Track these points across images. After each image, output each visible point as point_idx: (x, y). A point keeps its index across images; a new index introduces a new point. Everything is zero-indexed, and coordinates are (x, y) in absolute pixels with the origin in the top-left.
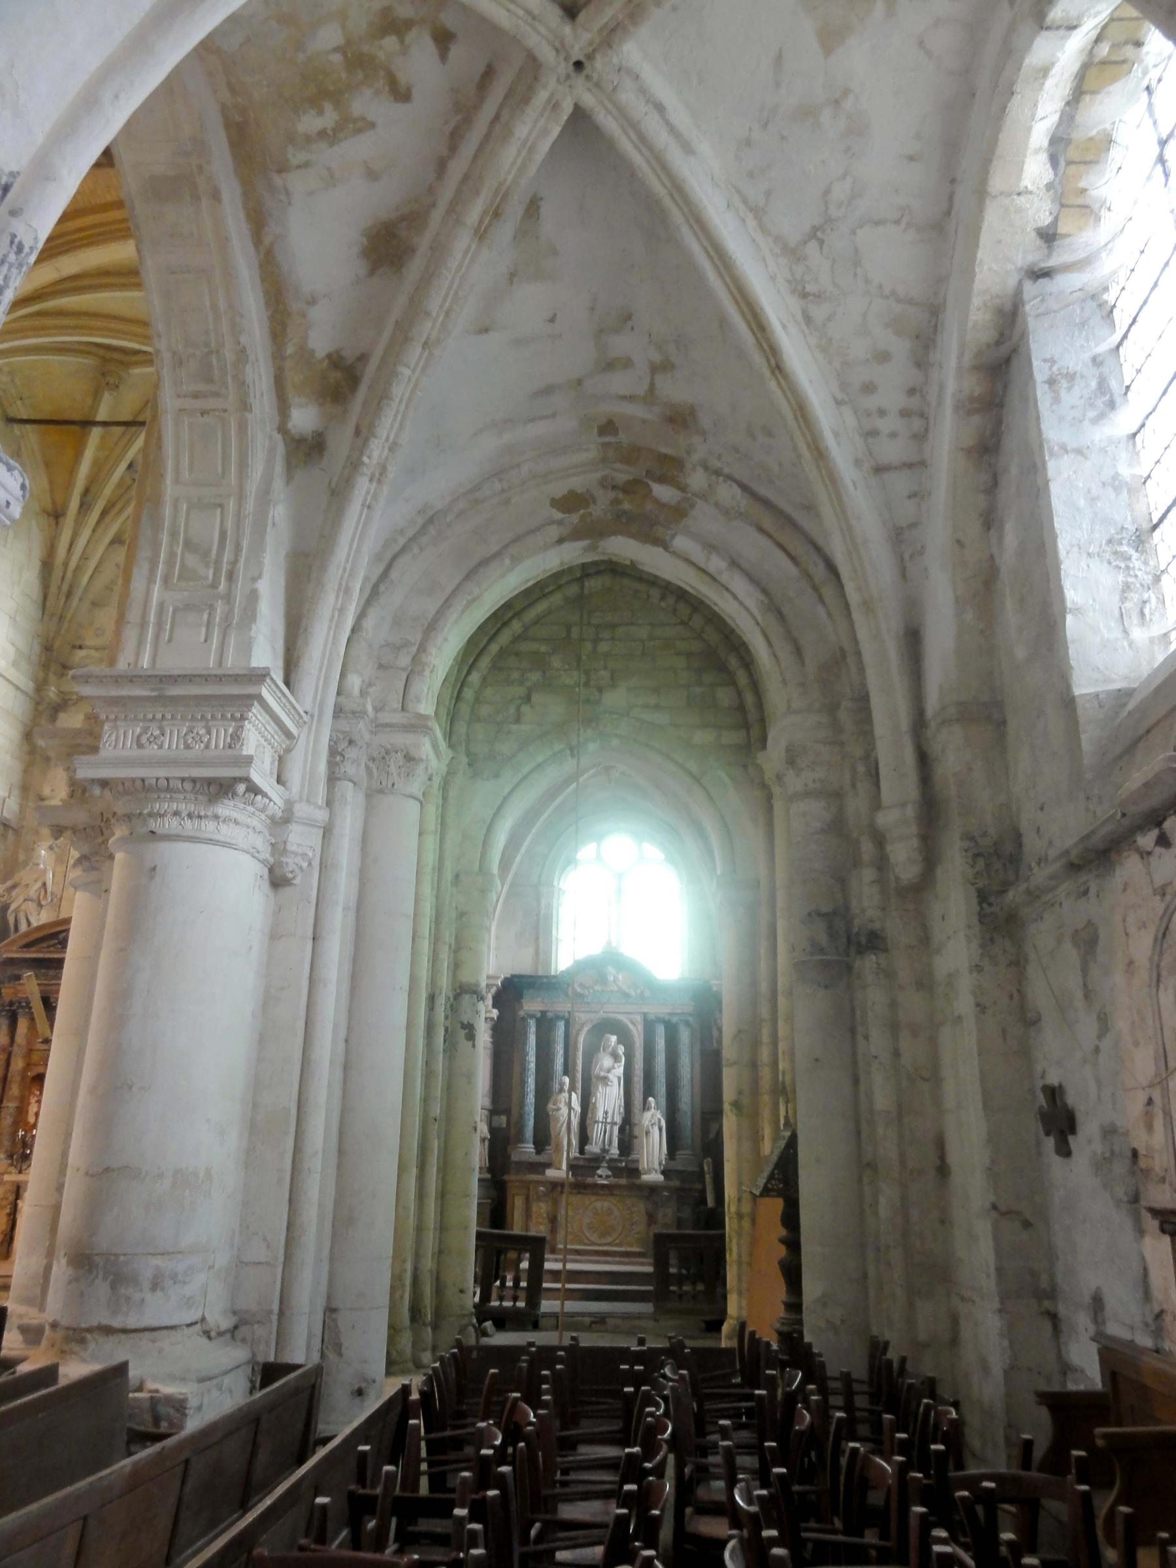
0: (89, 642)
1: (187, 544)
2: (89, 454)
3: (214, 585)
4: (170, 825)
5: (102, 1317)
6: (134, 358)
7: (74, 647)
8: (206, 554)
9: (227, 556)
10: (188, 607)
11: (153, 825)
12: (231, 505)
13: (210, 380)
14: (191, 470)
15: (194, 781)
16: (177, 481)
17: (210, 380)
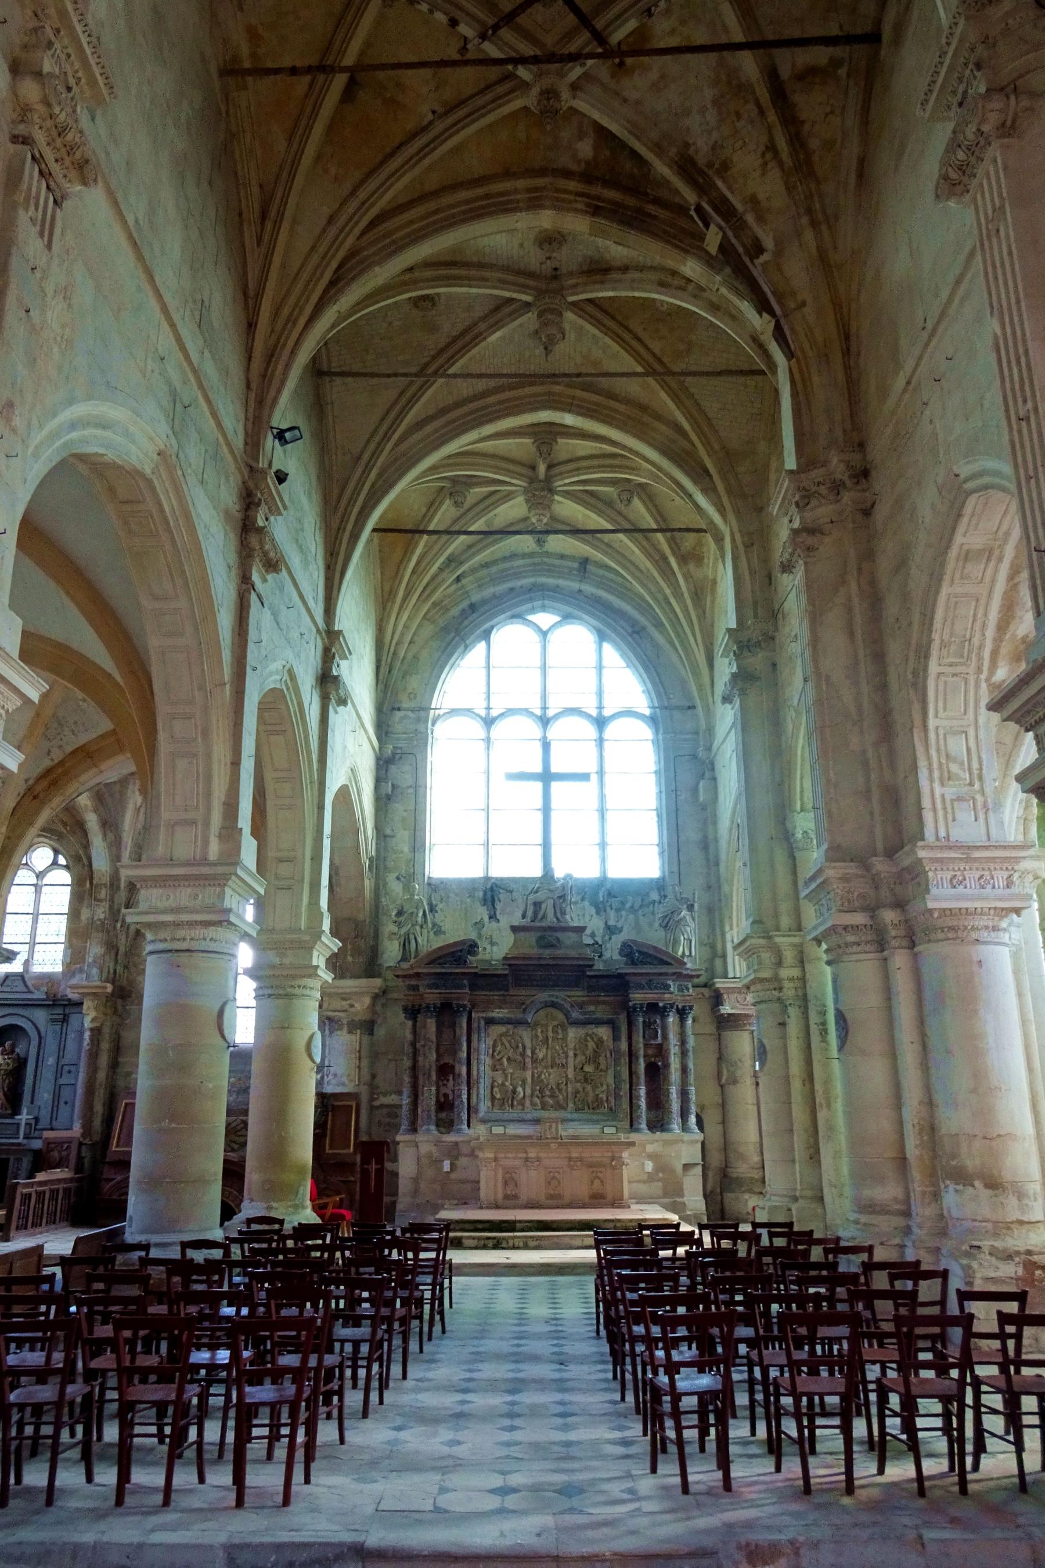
0: (404, 705)
1: (948, 756)
2: (418, 551)
3: (971, 784)
4: (984, 935)
5: (1014, 1215)
6: (474, 480)
7: (393, 709)
8: (962, 764)
9: (975, 765)
10: (960, 799)
11: (974, 935)
12: (971, 733)
13: (962, 657)
14: (945, 710)
15: (995, 908)
16: (936, 716)
17: (962, 657)
